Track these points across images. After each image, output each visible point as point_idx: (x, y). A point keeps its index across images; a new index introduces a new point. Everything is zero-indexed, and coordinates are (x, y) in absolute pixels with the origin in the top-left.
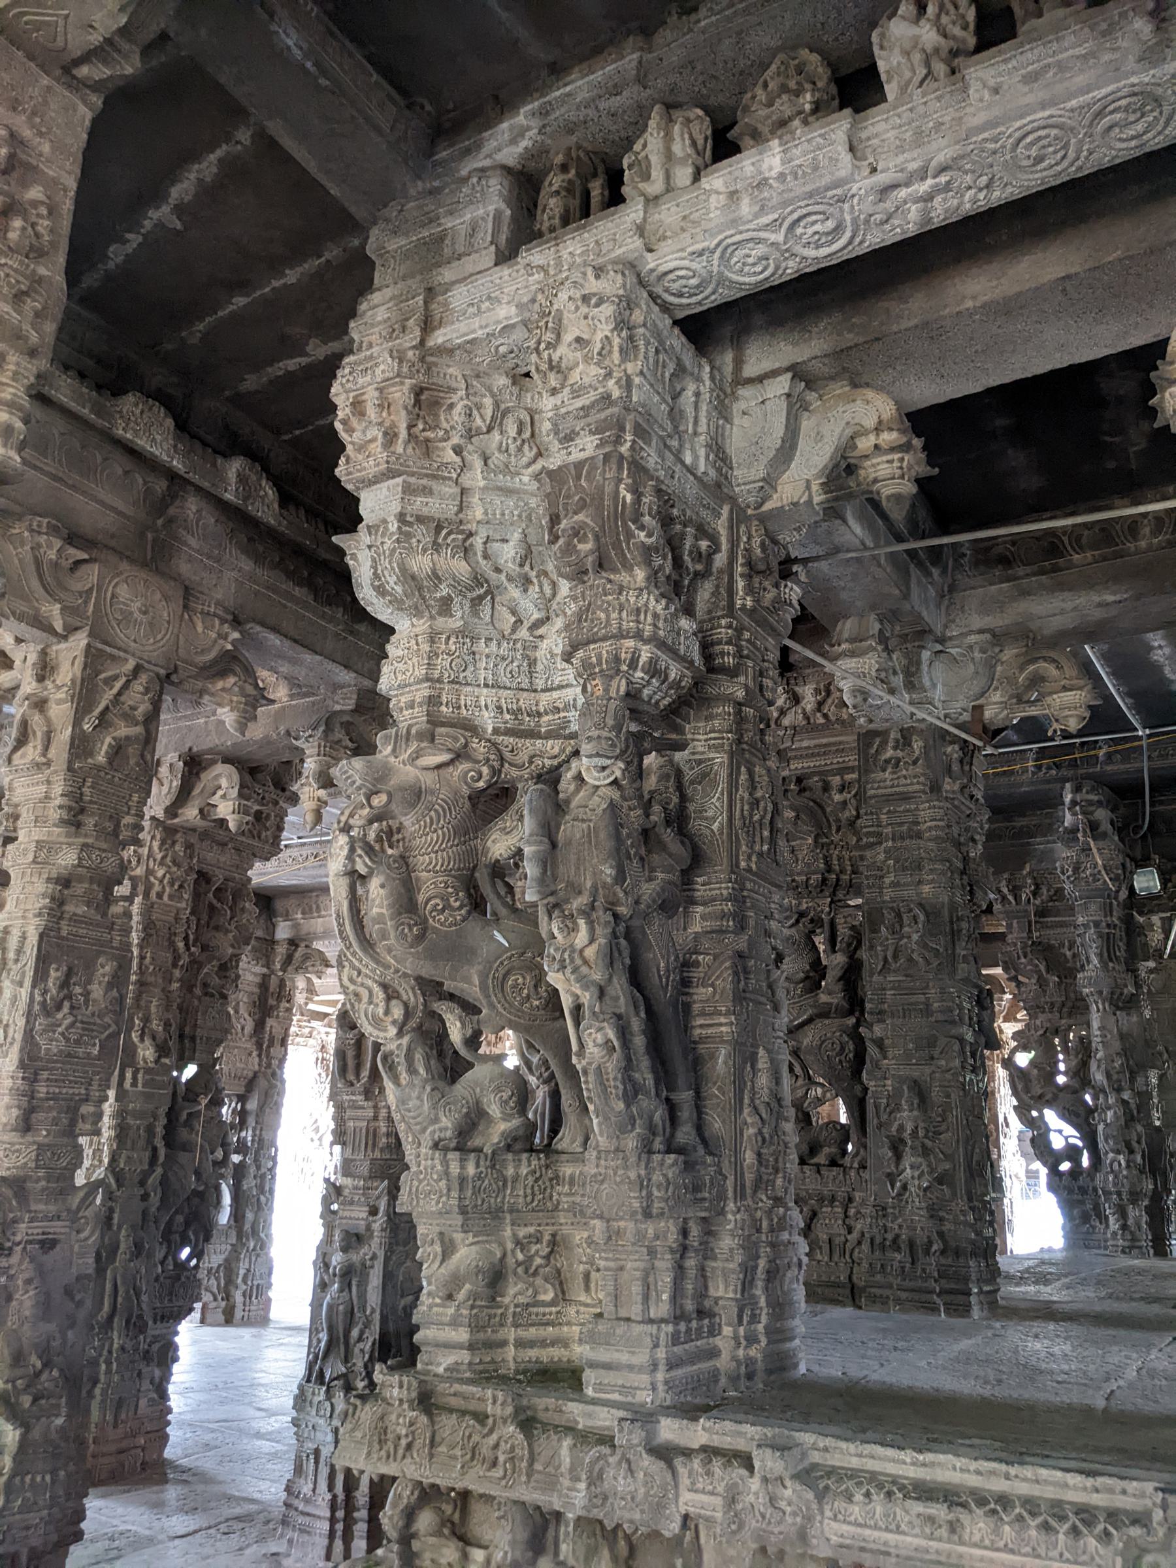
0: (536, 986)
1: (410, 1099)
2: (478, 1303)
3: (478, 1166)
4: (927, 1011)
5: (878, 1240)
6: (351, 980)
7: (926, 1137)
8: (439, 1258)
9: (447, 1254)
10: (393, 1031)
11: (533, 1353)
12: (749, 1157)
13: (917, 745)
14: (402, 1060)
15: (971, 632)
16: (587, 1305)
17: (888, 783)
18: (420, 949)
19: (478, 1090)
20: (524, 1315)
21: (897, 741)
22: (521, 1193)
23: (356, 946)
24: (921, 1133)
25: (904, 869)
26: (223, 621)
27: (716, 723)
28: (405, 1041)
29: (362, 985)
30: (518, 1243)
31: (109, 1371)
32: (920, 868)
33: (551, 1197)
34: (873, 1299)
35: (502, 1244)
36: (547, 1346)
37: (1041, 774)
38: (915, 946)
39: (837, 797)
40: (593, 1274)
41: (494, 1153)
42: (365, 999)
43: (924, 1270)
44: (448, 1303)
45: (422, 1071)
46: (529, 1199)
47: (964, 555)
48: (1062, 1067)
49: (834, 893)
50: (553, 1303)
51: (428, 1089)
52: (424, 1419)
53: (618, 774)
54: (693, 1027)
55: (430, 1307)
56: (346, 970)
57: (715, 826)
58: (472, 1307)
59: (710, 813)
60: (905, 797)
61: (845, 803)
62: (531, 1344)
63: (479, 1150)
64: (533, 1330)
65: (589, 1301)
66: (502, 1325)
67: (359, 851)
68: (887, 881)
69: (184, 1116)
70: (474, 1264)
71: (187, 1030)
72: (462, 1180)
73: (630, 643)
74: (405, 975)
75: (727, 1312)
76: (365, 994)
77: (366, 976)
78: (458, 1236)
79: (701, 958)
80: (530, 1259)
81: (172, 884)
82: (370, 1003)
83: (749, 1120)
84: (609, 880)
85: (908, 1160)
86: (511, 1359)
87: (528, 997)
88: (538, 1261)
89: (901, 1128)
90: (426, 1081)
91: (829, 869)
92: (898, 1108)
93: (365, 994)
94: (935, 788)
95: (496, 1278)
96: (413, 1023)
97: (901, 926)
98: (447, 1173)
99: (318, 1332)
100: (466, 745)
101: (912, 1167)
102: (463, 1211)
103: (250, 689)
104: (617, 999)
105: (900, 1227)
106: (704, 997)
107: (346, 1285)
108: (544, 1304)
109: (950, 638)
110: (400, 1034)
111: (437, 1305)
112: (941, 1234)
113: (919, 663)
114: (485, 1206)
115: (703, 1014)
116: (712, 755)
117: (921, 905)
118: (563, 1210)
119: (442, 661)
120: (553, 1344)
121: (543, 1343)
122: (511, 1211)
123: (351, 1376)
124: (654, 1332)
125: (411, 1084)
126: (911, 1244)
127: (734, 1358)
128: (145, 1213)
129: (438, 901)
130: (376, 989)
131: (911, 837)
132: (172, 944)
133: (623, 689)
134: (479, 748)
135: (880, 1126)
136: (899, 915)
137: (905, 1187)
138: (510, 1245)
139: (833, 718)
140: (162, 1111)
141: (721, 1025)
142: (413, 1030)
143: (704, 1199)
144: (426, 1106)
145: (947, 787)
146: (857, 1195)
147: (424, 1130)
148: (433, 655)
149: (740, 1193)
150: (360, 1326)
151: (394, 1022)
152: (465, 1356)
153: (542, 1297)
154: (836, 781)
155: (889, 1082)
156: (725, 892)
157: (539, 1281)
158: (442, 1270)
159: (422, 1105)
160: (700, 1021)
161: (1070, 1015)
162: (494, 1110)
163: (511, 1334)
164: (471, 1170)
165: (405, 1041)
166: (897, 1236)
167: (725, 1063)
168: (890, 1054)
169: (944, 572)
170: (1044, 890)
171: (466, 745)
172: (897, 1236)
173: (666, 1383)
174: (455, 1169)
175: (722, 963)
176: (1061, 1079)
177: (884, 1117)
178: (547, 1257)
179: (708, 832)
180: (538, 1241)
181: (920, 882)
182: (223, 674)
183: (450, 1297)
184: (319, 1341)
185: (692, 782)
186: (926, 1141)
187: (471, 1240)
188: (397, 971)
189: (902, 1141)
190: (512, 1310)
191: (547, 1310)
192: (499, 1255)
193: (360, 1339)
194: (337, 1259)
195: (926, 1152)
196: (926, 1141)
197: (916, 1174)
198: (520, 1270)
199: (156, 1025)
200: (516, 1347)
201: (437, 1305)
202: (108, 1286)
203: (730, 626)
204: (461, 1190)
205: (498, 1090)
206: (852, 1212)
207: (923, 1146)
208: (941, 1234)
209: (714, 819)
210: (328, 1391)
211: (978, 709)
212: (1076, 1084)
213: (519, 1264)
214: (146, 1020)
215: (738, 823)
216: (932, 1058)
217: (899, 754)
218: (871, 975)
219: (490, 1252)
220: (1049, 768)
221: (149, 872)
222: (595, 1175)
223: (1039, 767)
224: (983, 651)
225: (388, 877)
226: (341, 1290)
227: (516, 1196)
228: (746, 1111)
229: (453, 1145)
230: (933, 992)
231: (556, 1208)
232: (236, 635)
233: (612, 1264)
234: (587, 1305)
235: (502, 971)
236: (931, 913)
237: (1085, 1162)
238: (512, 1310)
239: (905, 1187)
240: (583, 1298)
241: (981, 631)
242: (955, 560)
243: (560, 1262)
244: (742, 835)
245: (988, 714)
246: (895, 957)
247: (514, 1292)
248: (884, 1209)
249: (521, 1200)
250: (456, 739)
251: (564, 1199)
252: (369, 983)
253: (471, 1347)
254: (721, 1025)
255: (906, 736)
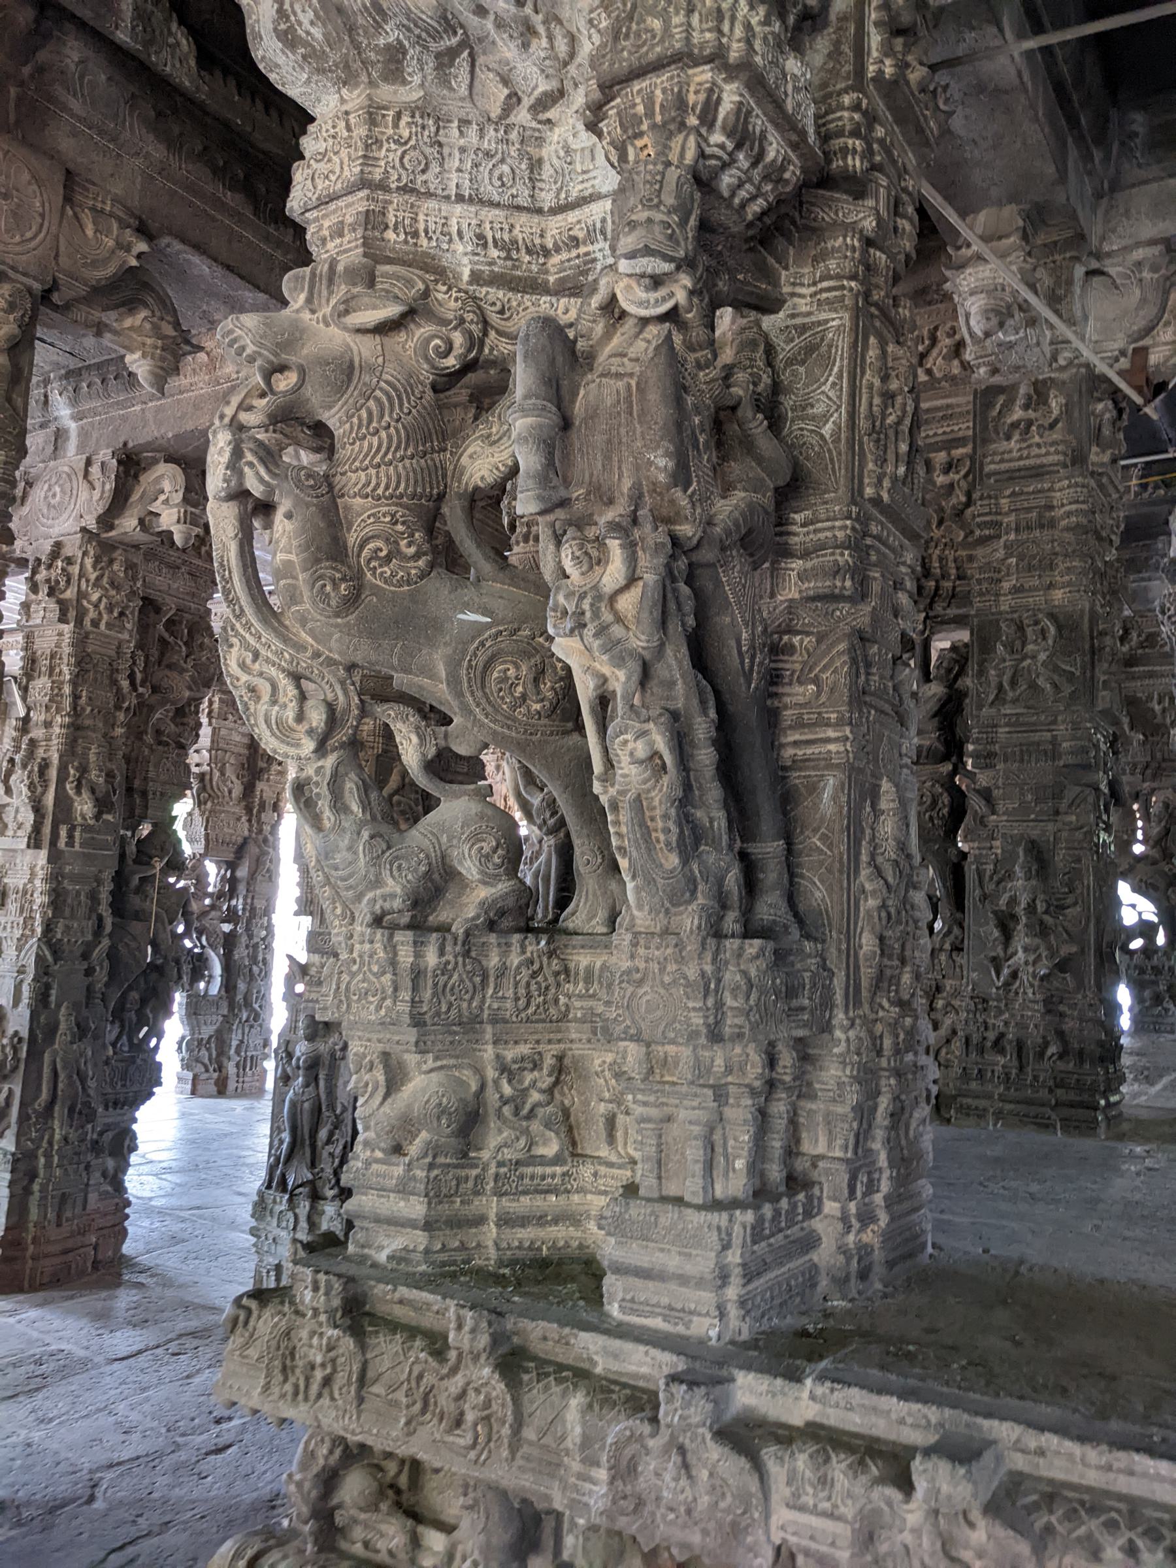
0: (536, 680)
1: (337, 849)
2: (441, 1160)
3: (442, 952)
4: (1053, 753)
5: (976, 1038)
6: (243, 666)
7: (1046, 912)
8: (382, 1091)
9: (393, 1084)
10: (309, 746)
11: (525, 1234)
12: (868, 943)
13: (1056, 403)
14: (324, 790)
15: (1138, 245)
16: (610, 1165)
17: (1015, 454)
18: (352, 618)
19: (444, 839)
20: (514, 1176)
21: (1029, 397)
22: (510, 993)
23: (249, 611)
24: (1040, 907)
25: (1030, 568)
26: (123, 225)
27: (832, 264)
28: (330, 761)
29: (261, 674)
30: (504, 1069)
31: (48, 1165)
32: (1051, 567)
33: (556, 1001)
34: (966, 1111)
35: (479, 1071)
36: (549, 1223)
37: (1146, 495)
38: (1042, 670)
39: (941, 480)
40: (621, 1119)
41: (467, 934)
42: (266, 698)
43: (1036, 1078)
44: (394, 1158)
45: (355, 807)
46: (522, 1003)
47: (1136, 134)
48: (1140, 835)
49: (931, 606)
50: (557, 1160)
51: (366, 835)
52: (348, 1343)
53: (681, 297)
54: (782, 746)
55: (368, 1163)
56: (235, 650)
57: (827, 430)
58: (431, 1166)
59: (819, 409)
60: (1038, 472)
61: (951, 485)
62: (523, 1221)
63: (444, 929)
64: (525, 1200)
65: (613, 1158)
66: (477, 1193)
67: (249, 457)
68: (1006, 585)
69: (135, 881)
70: (434, 1101)
71: (137, 783)
72: (417, 975)
73: (703, 75)
74: (330, 662)
75: (831, 1182)
76: (265, 689)
77: (267, 661)
78: (411, 1059)
79: (796, 640)
80: (524, 1093)
81: (110, 609)
82: (274, 702)
83: (868, 887)
84: (662, 477)
85: (1021, 939)
86: (490, 1243)
87: (524, 697)
88: (535, 1096)
89: (1013, 901)
90: (362, 824)
91: (927, 573)
92: (1010, 875)
93: (265, 689)
94: (1078, 459)
95: (469, 1121)
96: (342, 735)
97: (1024, 645)
98: (393, 963)
99: (280, 1131)
100: (426, 294)
101: (1026, 949)
102: (417, 1021)
103: (169, 330)
104: (672, 684)
105: (1006, 1023)
106: (801, 700)
107: (312, 1079)
108: (543, 1161)
109: (1109, 255)
110: (321, 749)
111: (377, 1161)
112: (1061, 1034)
113: (1070, 282)
114: (454, 1012)
115: (800, 725)
116: (823, 316)
117: (1052, 616)
118: (576, 1020)
119: (389, 154)
120: (556, 1221)
121: (541, 1220)
122: (494, 1021)
123: (319, 1184)
124: (724, 1223)
125: (339, 828)
126: (1020, 1046)
127: (843, 1250)
128: (89, 989)
129: (380, 544)
130: (284, 682)
131: (1042, 526)
132: (114, 682)
133: (690, 155)
134: (447, 302)
135: (984, 897)
136: (1021, 628)
137: (1014, 975)
138: (491, 1073)
139: (938, 375)
140: (108, 875)
141: (828, 740)
142: (343, 746)
143: (802, 1009)
144: (362, 861)
145: (1093, 458)
146: (949, 984)
147: (359, 898)
148: (372, 143)
149: (853, 997)
150: (329, 1127)
151: (310, 732)
152: (420, 1239)
153: (540, 1151)
154: (941, 457)
155: (997, 843)
156: (840, 535)
157: (535, 1126)
158: (386, 1108)
159: (356, 860)
160: (796, 736)
161: (1154, 777)
162: (469, 868)
163: (491, 1206)
164: (431, 959)
165: (330, 761)
166: (1002, 1036)
167: (835, 798)
168: (1000, 808)
169: (1107, 158)
170: (1134, 635)
171: (426, 294)
172: (1002, 1036)
173: (742, 1303)
174: (406, 957)
175: (833, 645)
176: (1138, 849)
177: (990, 887)
178: (550, 1091)
179: (814, 440)
180: (536, 1066)
181: (1051, 586)
182: (130, 305)
183: (398, 1150)
184: (281, 1142)
185: (790, 362)
186: (1046, 918)
187: (431, 1064)
188: (317, 655)
189: (1014, 917)
190: (492, 1170)
191: (549, 1170)
192: (474, 1087)
193: (329, 1141)
194: (301, 1049)
195: (1043, 931)
196: (1046, 918)
197: (1031, 958)
198: (507, 1110)
199: (94, 775)
200: (498, 1225)
201: (377, 1161)
202: (46, 1071)
203: (856, 107)
204: (415, 989)
205: (476, 838)
206: (940, 1004)
207: (1041, 922)
208: (1061, 1034)
209: (825, 418)
210: (290, 1200)
211: (1141, 353)
212: (1155, 853)
213: (505, 1101)
214: (83, 770)
215: (863, 424)
216: (1057, 813)
217: (1031, 414)
218: (980, 707)
219: (462, 1083)
220: (1156, 487)
221: (81, 595)
222: (628, 972)
223: (1144, 487)
224: (1154, 269)
225: (298, 502)
226: (306, 1085)
227: (501, 999)
228: (865, 872)
229: (405, 919)
230: (1062, 729)
231: (564, 1017)
232: (142, 247)
233: (653, 1112)
234: (610, 1165)
235: (482, 658)
236: (1065, 624)
237: (1161, 939)
238: (492, 1170)
239: (1014, 975)
240: (604, 1152)
241: (1152, 242)
242: (1123, 144)
243: (571, 1098)
244: (869, 445)
245: (1154, 358)
246: (1013, 683)
247: (497, 1143)
248: (985, 1001)
249: (509, 1004)
250: (409, 283)
251: (578, 1004)
252: (273, 671)
253: (428, 1226)
254: (828, 740)
255: (1039, 393)
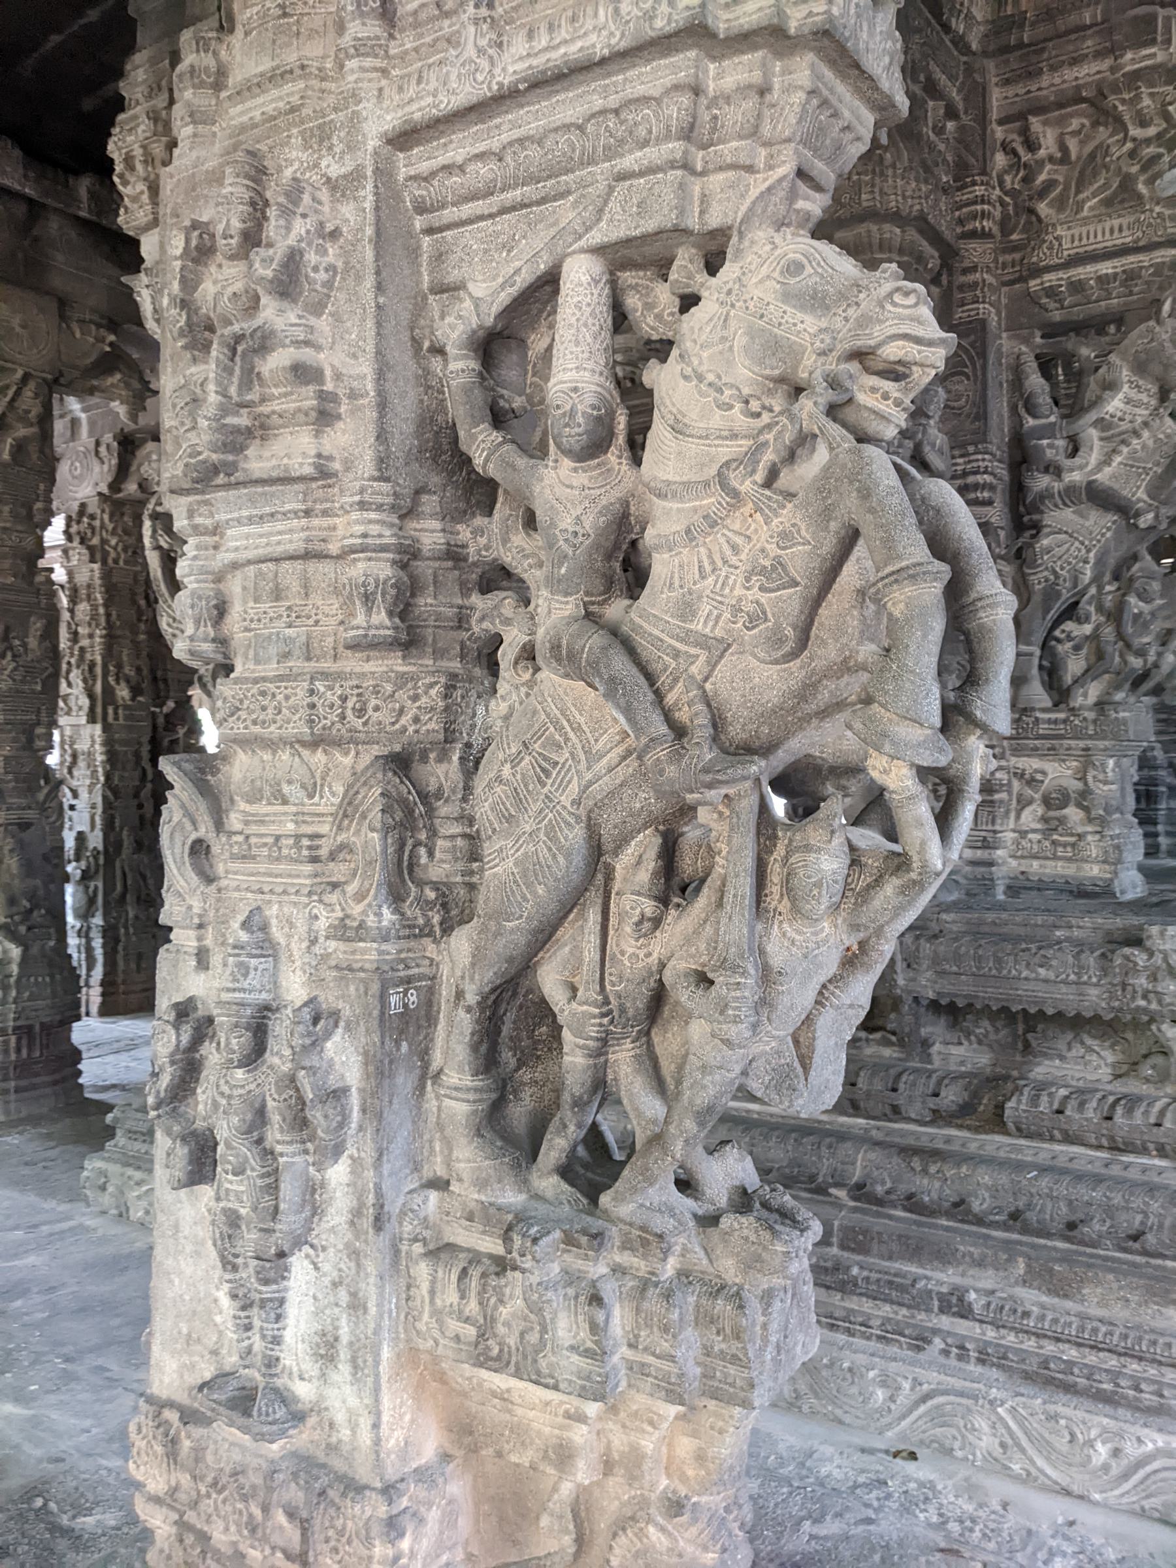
26: (99, 326)
69: (166, 742)
71: (159, 674)
81: (125, 550)
103: (136, 385)
128: (142, 818)
132: (134, 602)
140: (145, 739)
182: (110, 371)
199: (128, 670)
214: (119, 666)
221: (104, 542)
232: (112, 338)
